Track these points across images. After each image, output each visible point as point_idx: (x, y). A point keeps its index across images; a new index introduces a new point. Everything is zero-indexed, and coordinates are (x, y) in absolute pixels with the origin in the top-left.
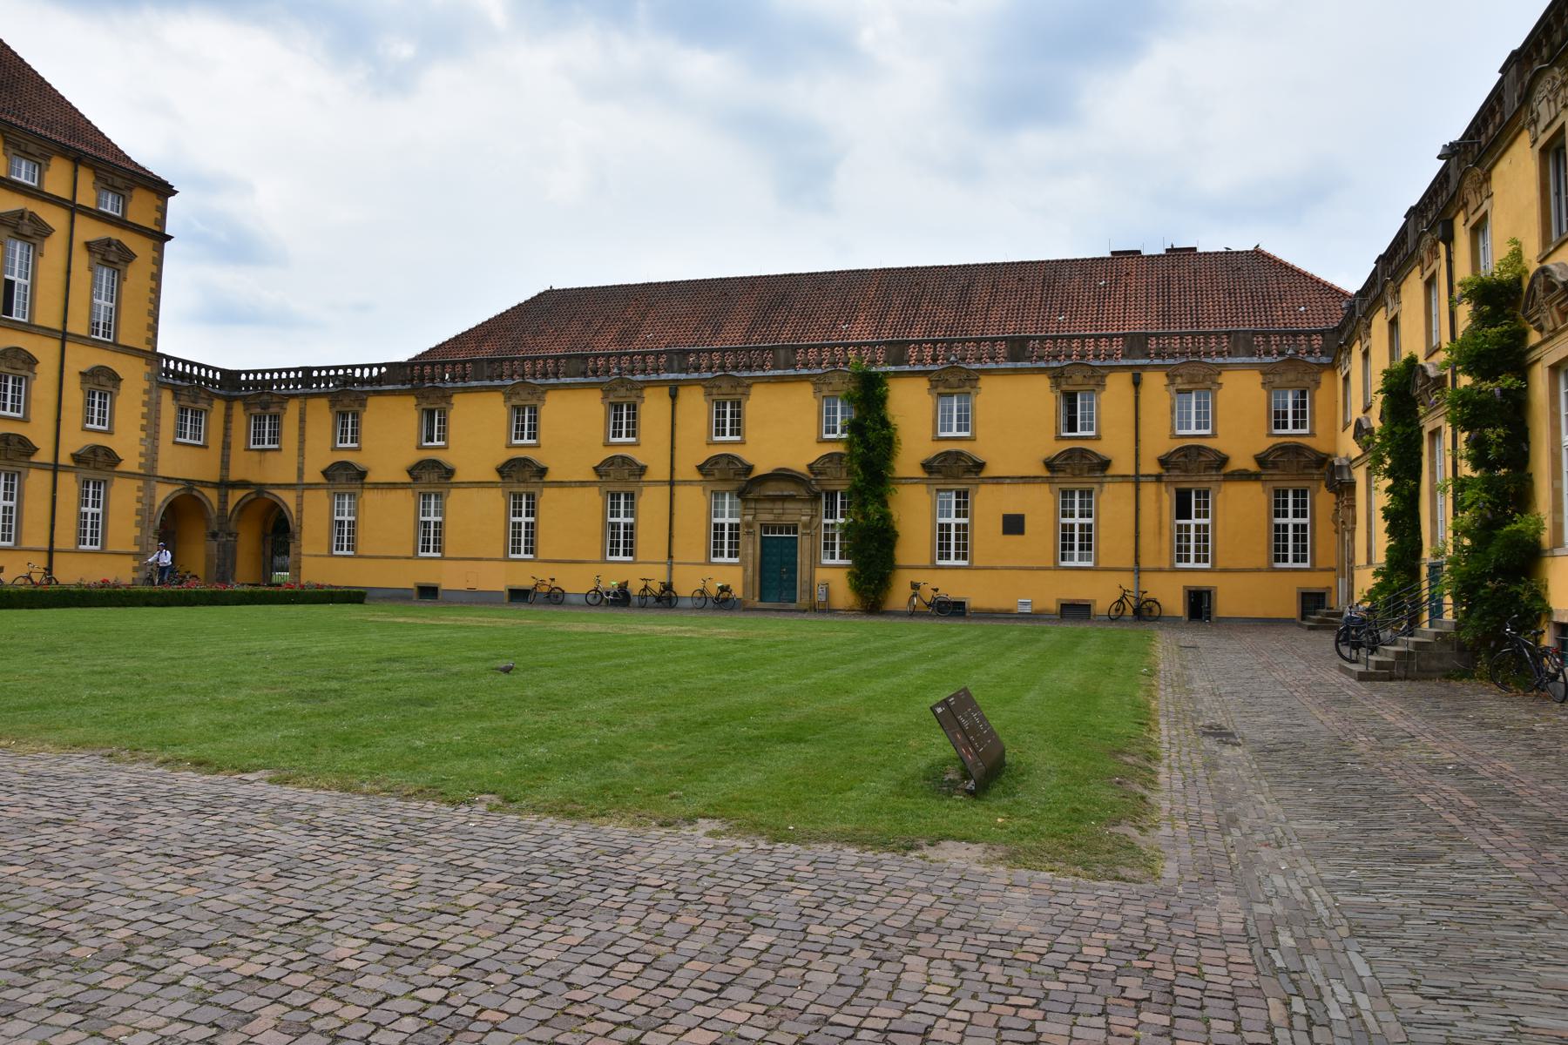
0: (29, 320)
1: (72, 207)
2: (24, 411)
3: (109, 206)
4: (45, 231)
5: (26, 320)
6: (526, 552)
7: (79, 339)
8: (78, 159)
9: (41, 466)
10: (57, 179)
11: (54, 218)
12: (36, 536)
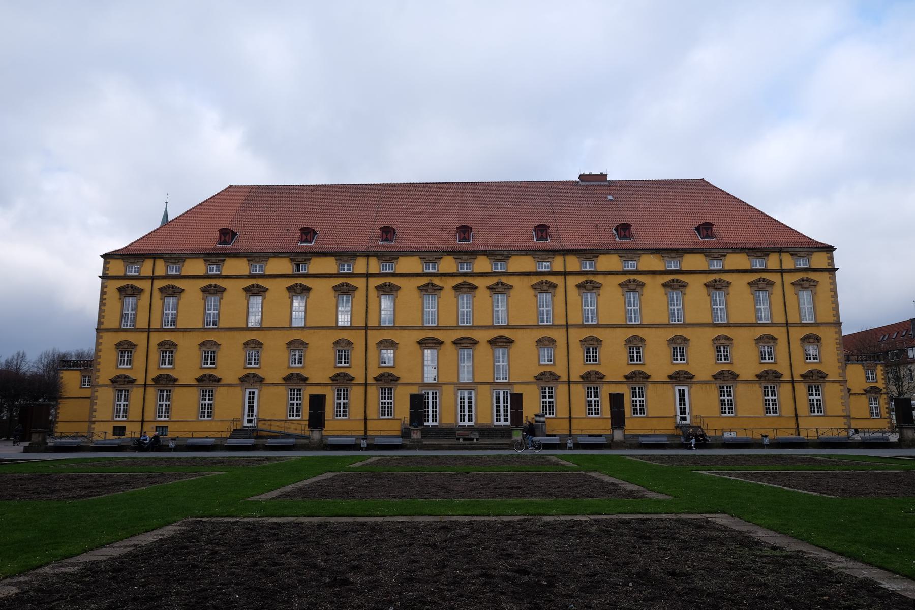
1: (782, 271)
3: (802, 264)
4: (771, 284)
5: (770, 322)
7: (795, 325)
8: (780, 250)
9: (787, 382)
10: (773, 262)
11: (775, 278)
12: (786, 409)
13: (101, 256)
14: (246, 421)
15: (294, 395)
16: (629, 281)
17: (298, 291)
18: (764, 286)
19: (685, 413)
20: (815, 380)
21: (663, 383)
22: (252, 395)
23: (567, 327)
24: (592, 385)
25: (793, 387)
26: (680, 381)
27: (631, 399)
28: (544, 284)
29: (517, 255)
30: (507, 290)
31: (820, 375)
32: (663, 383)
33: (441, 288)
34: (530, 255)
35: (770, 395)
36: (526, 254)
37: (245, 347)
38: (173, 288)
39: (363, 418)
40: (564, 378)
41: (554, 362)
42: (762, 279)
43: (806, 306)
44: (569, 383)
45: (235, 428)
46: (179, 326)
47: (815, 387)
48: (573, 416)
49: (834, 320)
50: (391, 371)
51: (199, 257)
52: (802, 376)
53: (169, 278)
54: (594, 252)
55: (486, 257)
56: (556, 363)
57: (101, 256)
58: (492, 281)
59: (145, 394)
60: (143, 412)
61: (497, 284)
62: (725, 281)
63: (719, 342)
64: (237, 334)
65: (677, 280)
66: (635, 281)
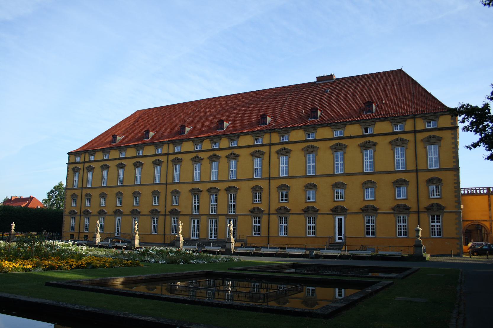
0: (406, 169)
2: (407, 196)
6: (258, 234)
10: (409, 125)
11: (409, 137)
13: (68, 154)
14: (116, 234)
15: (283, 221)
16: (309, 146)
17: (105, 168)
18: (401, 143)
19: (341, 235)
20: (436, 211)
21: (327, 214)
22: (119, 220)
23: (269, 179)
24: (283, 216)
25: (419, 217)
26: (338, 213)
27: (316, 225)
28: (257, 152)
29: (243, 135)
30: (237, 157)
31: (439, 207)
32: (327, 214)
33: (202, 159)
34: (250, 135)
35: (402, 222)
36: (248, 135)
37: (116, 196)
38: (91, 167)
39: (164, 234)
40: (267, 212)
41: (261, 202)
42: (399, 139)
43: (433, 156)
44: (269, 214)
45: (107, 237)
46: (124, 184)
47: (437, 217)
48: (270, 235)
49: (454, 166)
50: (313, 205)
51: (100, 151)
52: (426, 208)
53: (90, 162)
54: (288, 129)
55: (226, 138)
56: (346, 200)
57: (68, 154)
58: (228, 152)
59: (80, 219)
60: (79, 228)
61: (231, 154)
62: (373, 142)
63: (367, 185)
64: (113, 189)
65: (340, 144)
66: (312, 146)
